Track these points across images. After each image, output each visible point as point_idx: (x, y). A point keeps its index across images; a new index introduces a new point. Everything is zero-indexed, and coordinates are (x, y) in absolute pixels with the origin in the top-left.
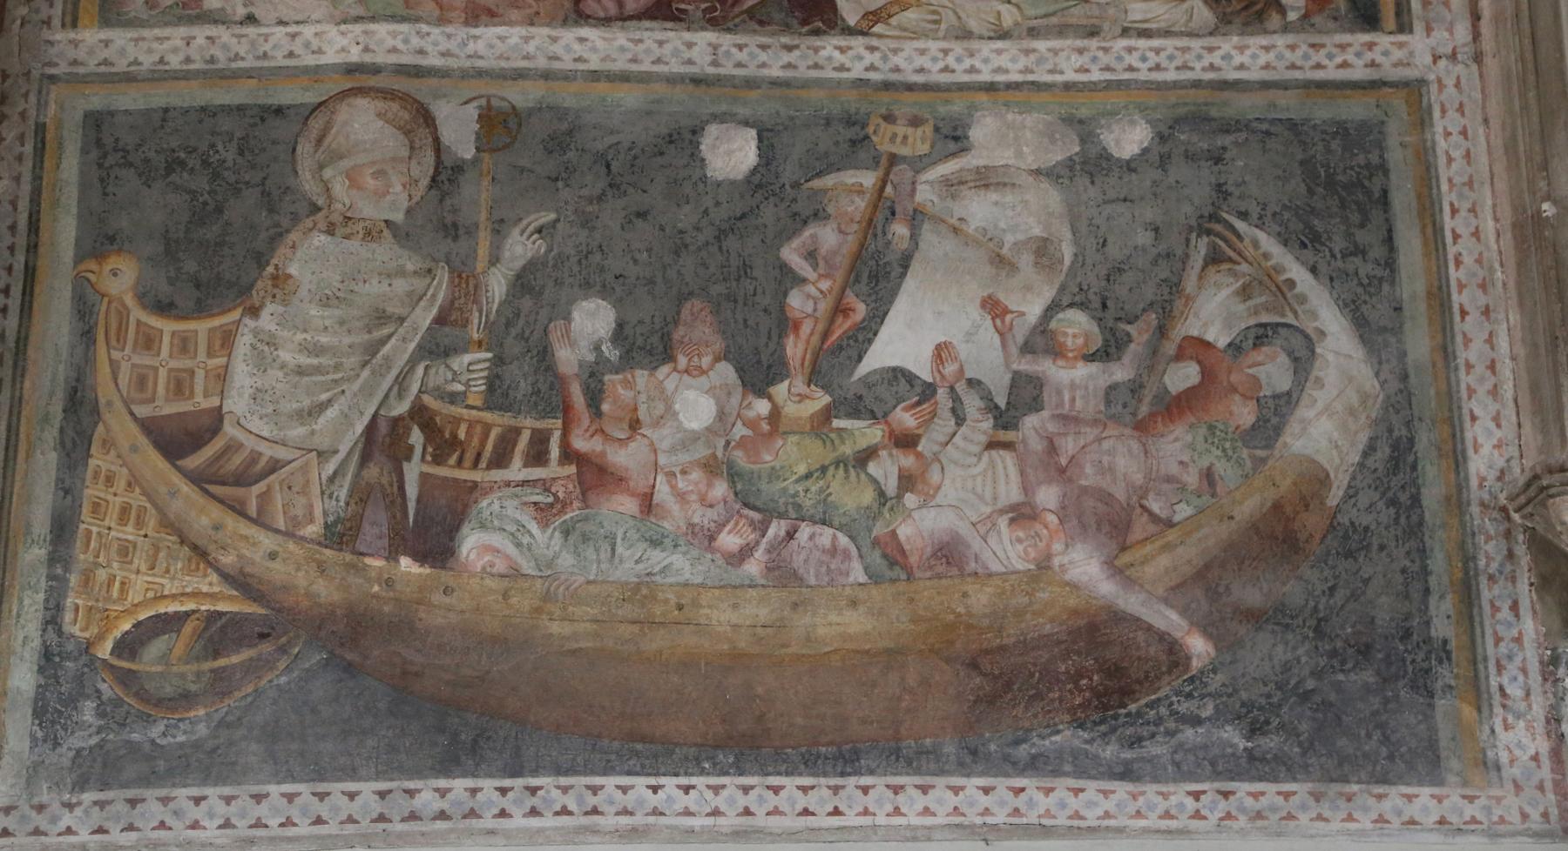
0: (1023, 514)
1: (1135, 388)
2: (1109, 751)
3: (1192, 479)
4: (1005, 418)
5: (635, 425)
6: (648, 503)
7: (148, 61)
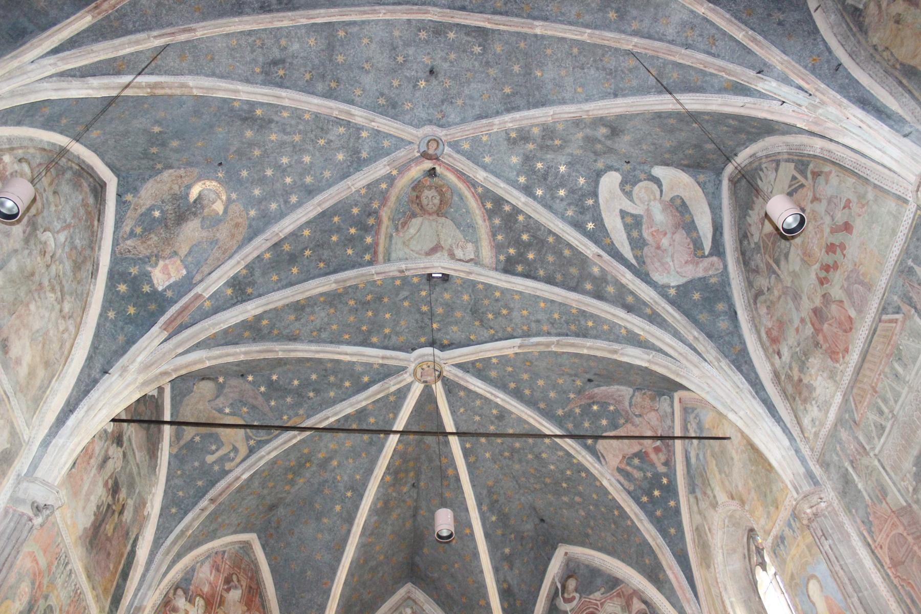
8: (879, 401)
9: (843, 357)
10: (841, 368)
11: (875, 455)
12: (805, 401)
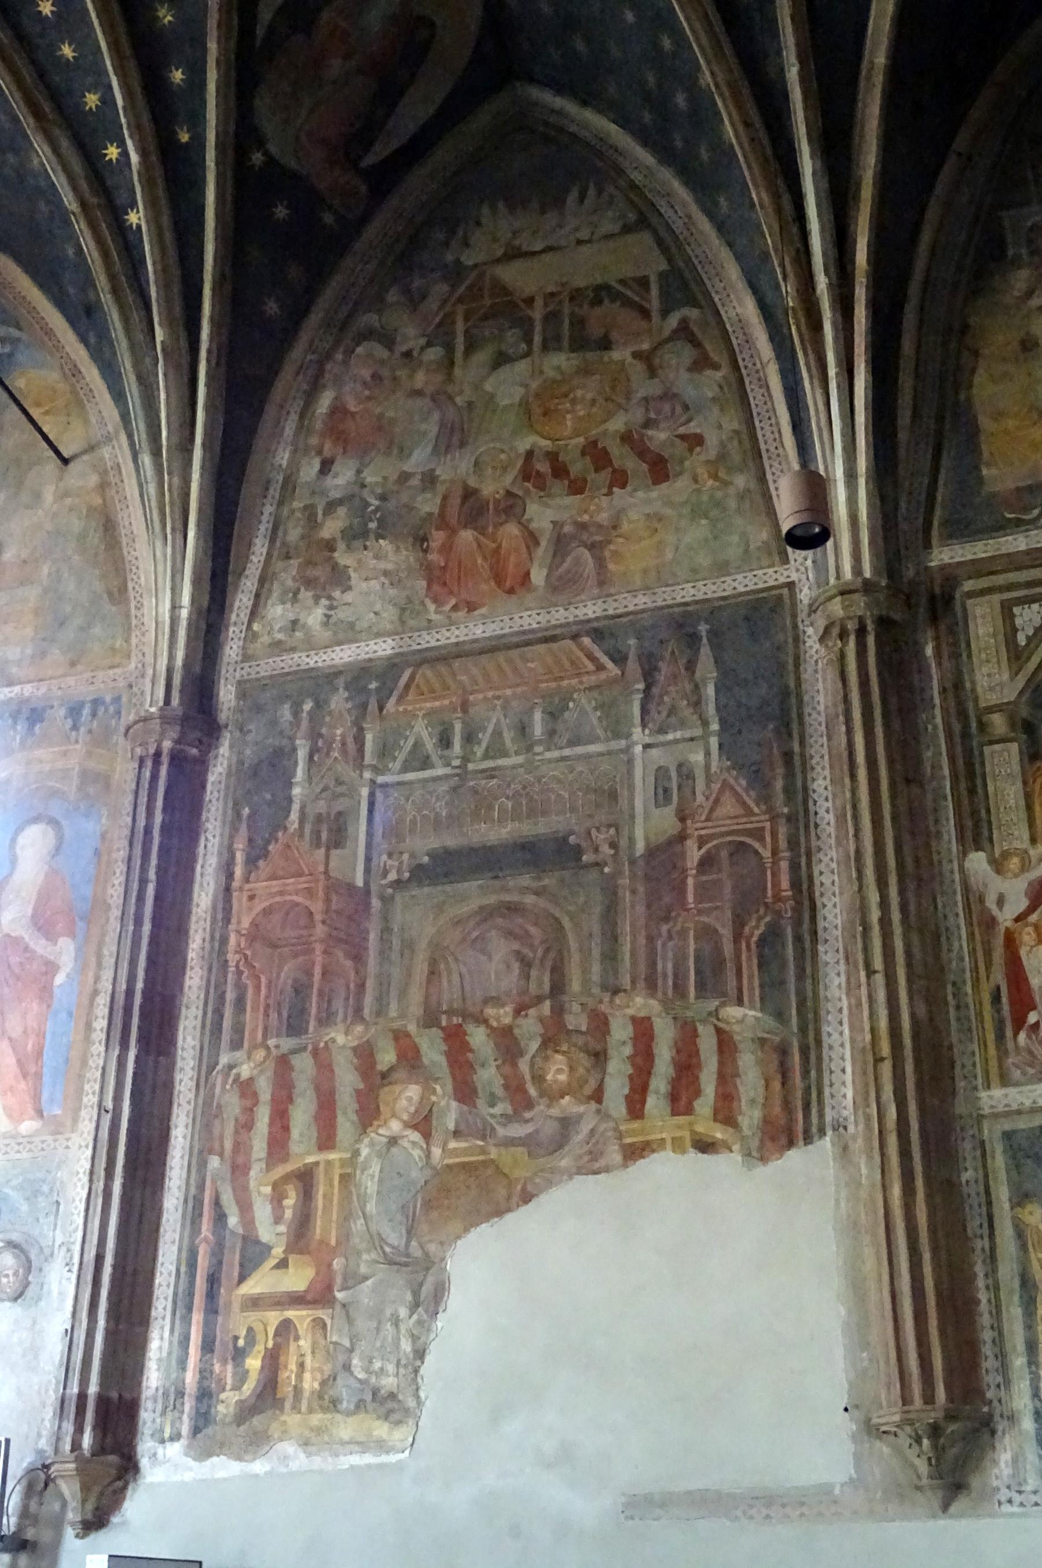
7: (1028, 1103)
8: (458, 727)
9: (455, 608)
10: (433, 616)
11: (373, 782)
12: (309, 583)
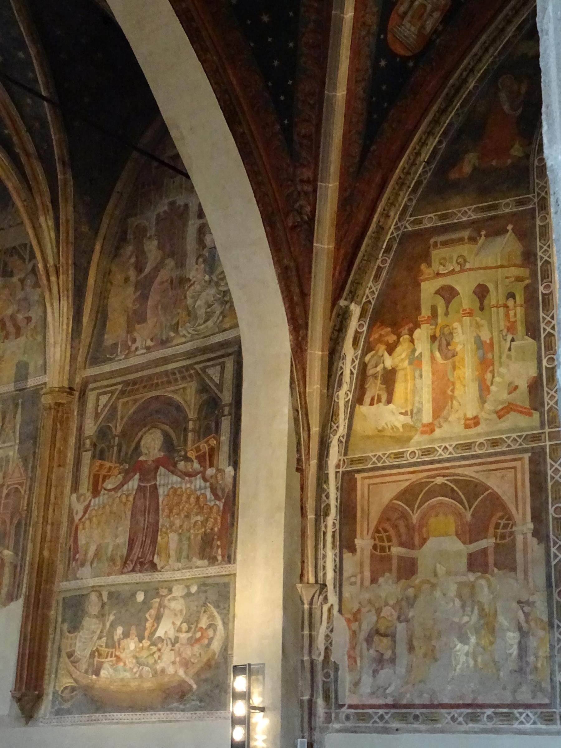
0: (174, 663)
1: (192, 637)
2: (182, 706)
3: (198, 655)
4: (173, 645)
5: (124, 649)
6: (125, 664)
